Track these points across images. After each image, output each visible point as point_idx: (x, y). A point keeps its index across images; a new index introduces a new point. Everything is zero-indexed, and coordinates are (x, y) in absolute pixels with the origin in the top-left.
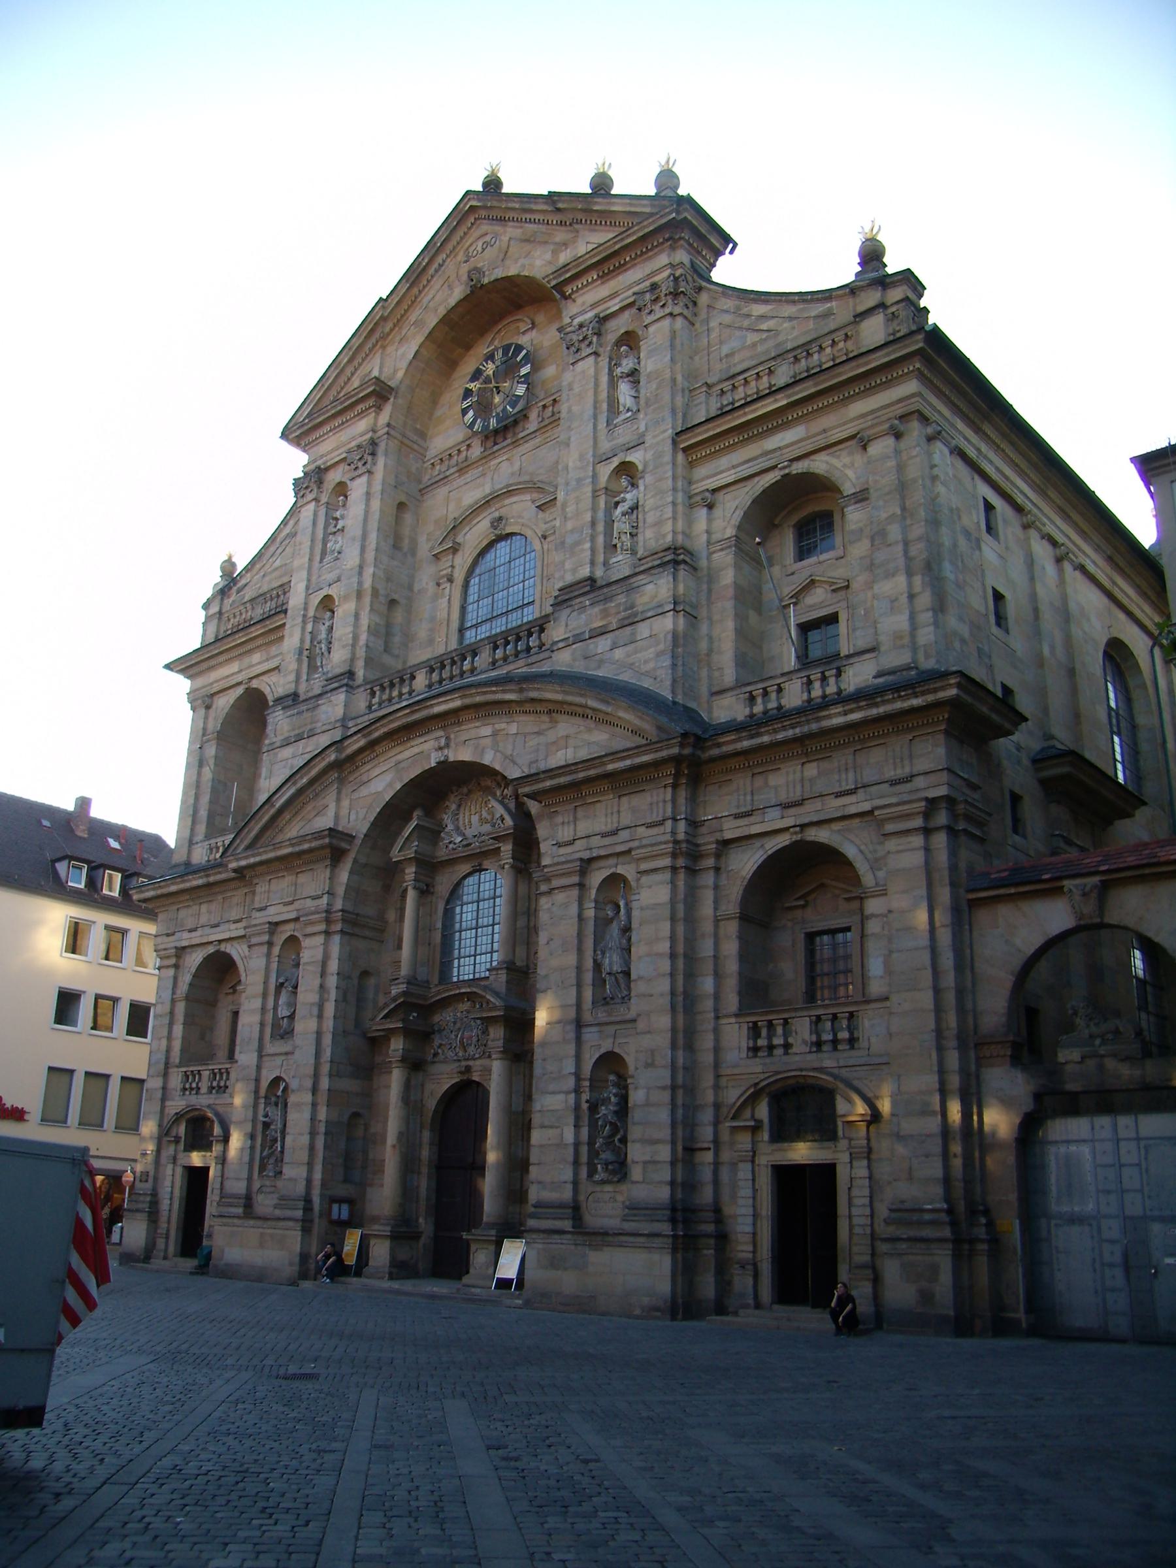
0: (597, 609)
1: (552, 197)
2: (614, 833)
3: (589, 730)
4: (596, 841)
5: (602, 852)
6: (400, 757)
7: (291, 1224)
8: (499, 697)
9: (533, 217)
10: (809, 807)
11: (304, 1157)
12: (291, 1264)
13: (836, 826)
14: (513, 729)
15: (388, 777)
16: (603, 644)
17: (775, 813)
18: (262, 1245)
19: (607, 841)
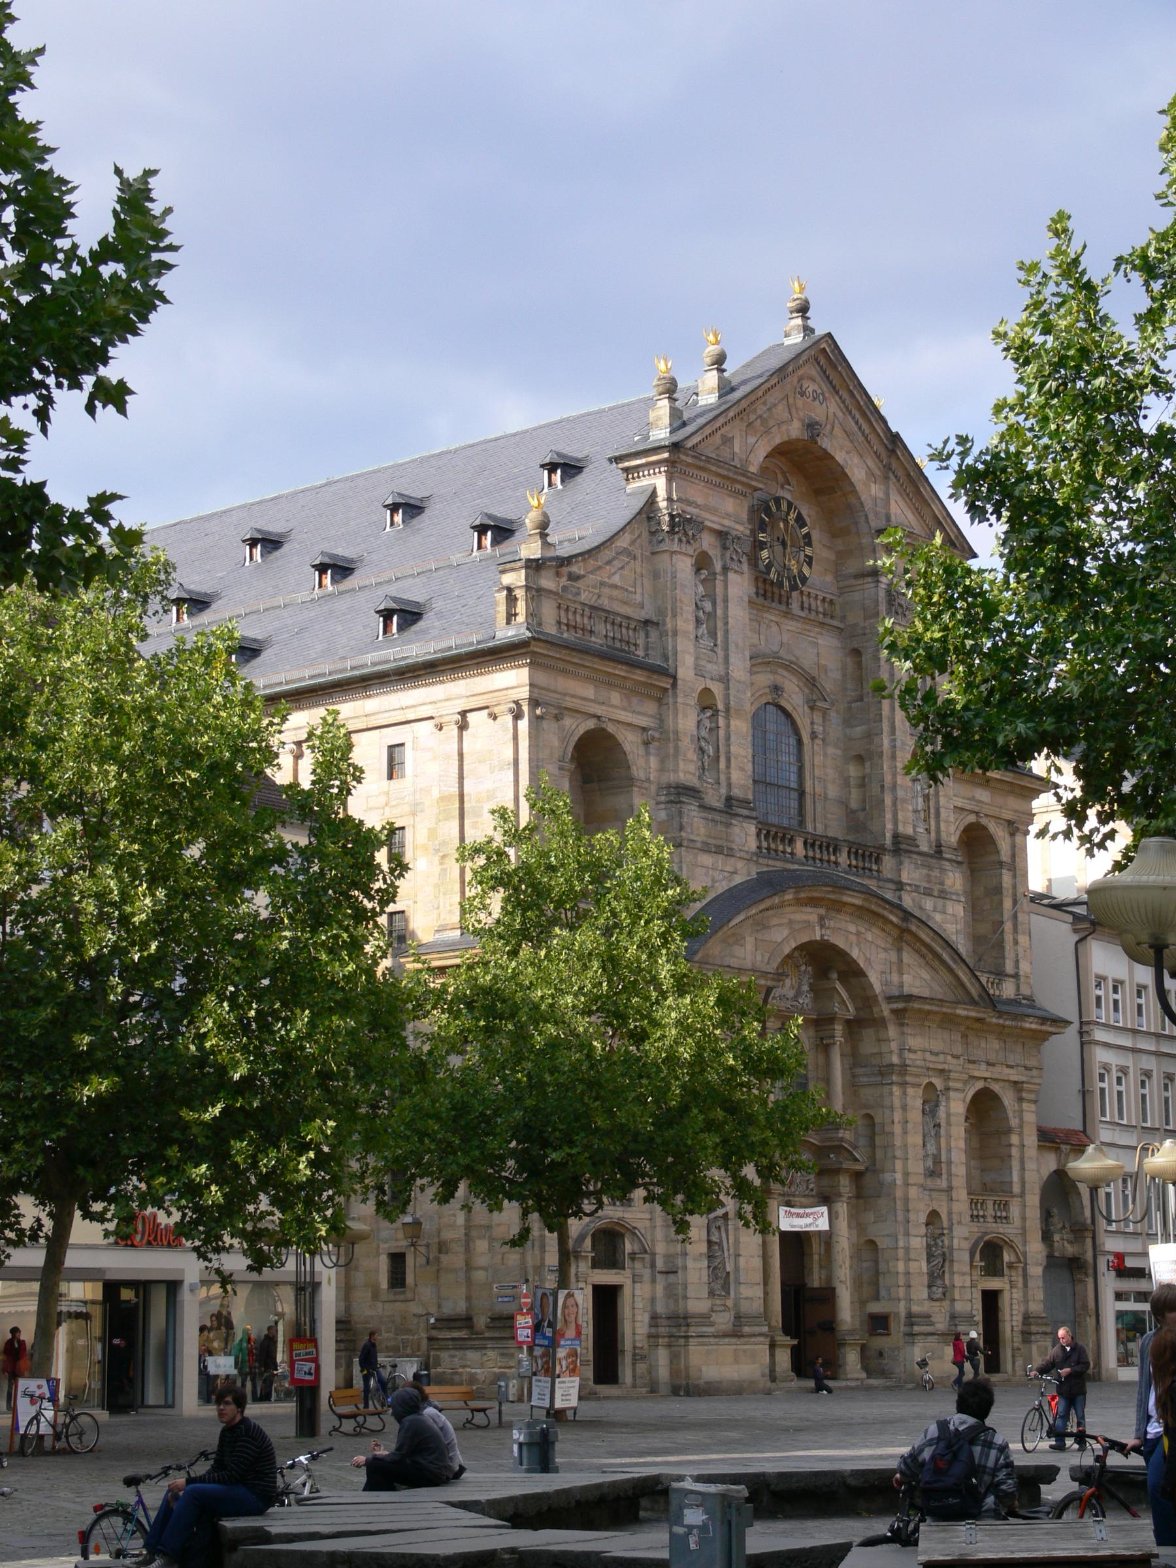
0: (925, 871)
1: (896, 438)
2: (937, 1054)
3: (920, 966)
4: (928, 1056)
5: (931, 1066)
6: (793, 917)
7: (761, 1339)
8: (886, 913)
9: (861, 421)
10: (998, 1069)
11: (758, 1277)
12: (763, 1376)
13: (1002, 1084)
14: (869, 937)
15: (786, 932)
16: (929, 904)
17: (983, 1066)
18: (736, 1361)
19: (933, 1058)
